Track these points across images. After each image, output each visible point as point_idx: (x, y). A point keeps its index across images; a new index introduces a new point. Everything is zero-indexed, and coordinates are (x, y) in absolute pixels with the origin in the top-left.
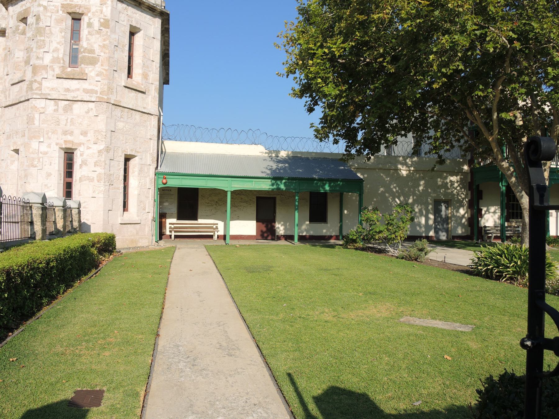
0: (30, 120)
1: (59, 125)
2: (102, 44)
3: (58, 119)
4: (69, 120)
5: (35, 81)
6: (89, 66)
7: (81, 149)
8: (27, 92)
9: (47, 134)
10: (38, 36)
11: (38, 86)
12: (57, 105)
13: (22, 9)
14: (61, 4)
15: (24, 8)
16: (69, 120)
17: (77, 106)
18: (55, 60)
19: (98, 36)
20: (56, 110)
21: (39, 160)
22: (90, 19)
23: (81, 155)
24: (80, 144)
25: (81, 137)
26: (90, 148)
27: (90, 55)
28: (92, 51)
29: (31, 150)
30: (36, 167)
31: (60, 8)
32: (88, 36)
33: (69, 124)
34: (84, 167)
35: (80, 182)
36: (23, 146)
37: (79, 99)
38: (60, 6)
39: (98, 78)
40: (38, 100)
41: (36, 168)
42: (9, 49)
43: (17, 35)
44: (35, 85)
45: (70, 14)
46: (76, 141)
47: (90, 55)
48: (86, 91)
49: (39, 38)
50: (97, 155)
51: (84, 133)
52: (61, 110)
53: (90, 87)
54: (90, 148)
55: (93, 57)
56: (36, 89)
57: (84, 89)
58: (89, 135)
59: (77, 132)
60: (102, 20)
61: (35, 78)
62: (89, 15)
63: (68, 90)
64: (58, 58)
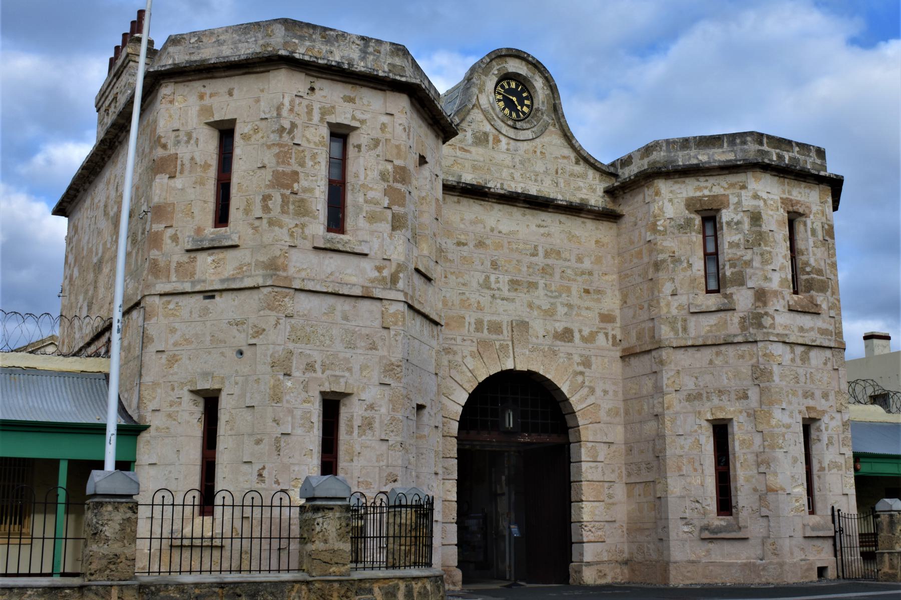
0: (760, 375)
1: (798, 383)
2: (830, 262)
3: (796, 373)
4: (808, 375)
5: (766, 314)
6: (820, 294)
7: (826, 419)
8: (743, 328)
9: (788, 396)
10: (762, 244)
11: (772, 322)
12: (793, 352)
13: (698, 194)
14: (781, 198)
15: (707, 192)
16: (808, 375)
17: (813, 353)
18: (782, 282)
19: (823, 249)
20: (793, 360)
21: (784, 436)
22: (813, 223)
23: (827, 429)
24: (824, 412)
25: (823, 401)
26: (834, 418)
27: (819, 277)
28: (819, 272)
29: (773, 422)
30: (781, 448)
31: (779, 204)
32: (814, 249)
33: (808, 381)
34: (831, 449)
35: (829, 471)
36: (745, 414)
37: (817, 343)
38: (779, 201)
39: (832, 313)
40: (775, 345)
41: (782, 450)
42: (674, 252)
43: (694, 234)
44: (767, 321)
45: (789, 212)
46: (819, 408)
47: (819, 277)
48: (823, 332)
49: (764, 248)
50: (841, 429)
51: (825, 396)
52: (798, 360)
53: (825, 326)
54: (834, 418)
55: (822, 280)
56: (770, 328)
57: (818, 328)
58: (830, 398)
59: (818, 394)
60: (826, 227)
61: (767, 310)
62: (812, 216)
63: (801, 329)
64: (786, 279)
